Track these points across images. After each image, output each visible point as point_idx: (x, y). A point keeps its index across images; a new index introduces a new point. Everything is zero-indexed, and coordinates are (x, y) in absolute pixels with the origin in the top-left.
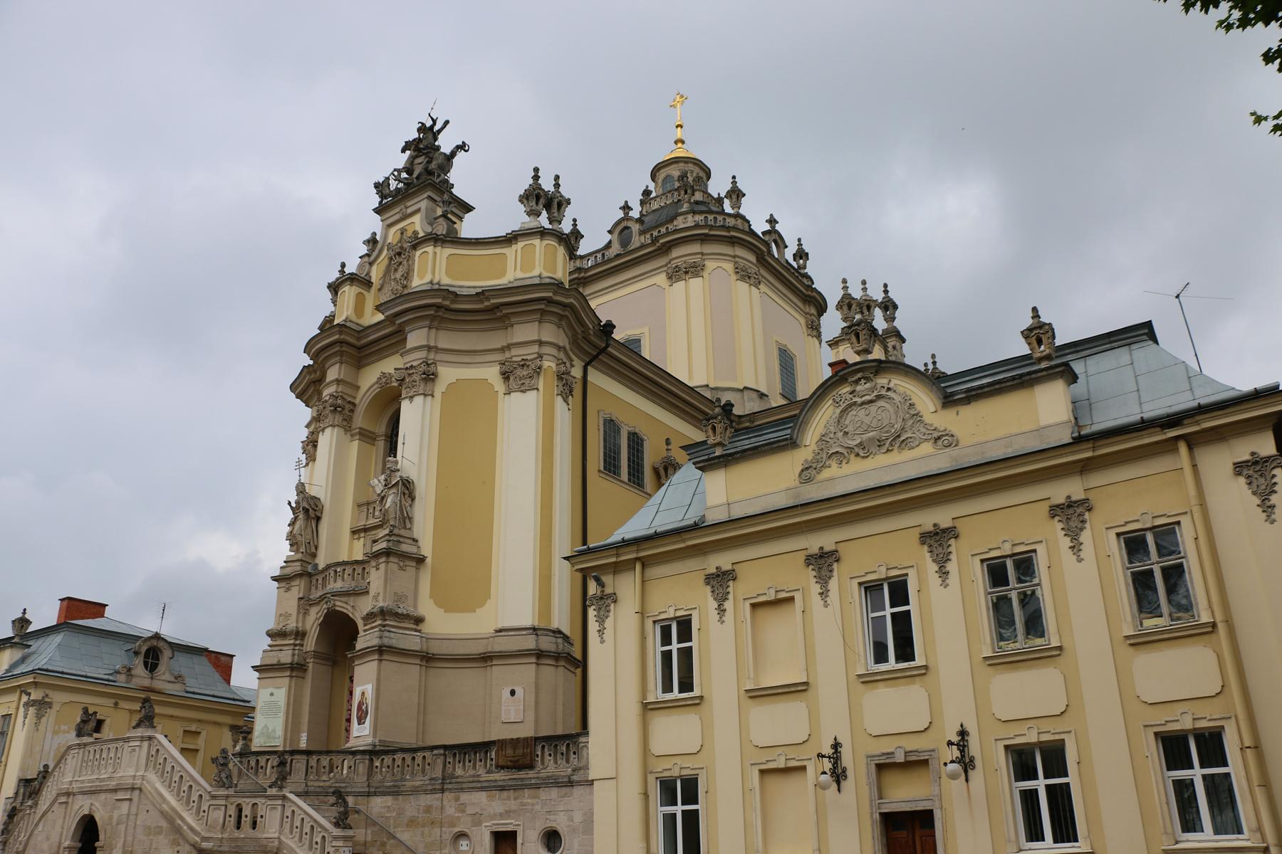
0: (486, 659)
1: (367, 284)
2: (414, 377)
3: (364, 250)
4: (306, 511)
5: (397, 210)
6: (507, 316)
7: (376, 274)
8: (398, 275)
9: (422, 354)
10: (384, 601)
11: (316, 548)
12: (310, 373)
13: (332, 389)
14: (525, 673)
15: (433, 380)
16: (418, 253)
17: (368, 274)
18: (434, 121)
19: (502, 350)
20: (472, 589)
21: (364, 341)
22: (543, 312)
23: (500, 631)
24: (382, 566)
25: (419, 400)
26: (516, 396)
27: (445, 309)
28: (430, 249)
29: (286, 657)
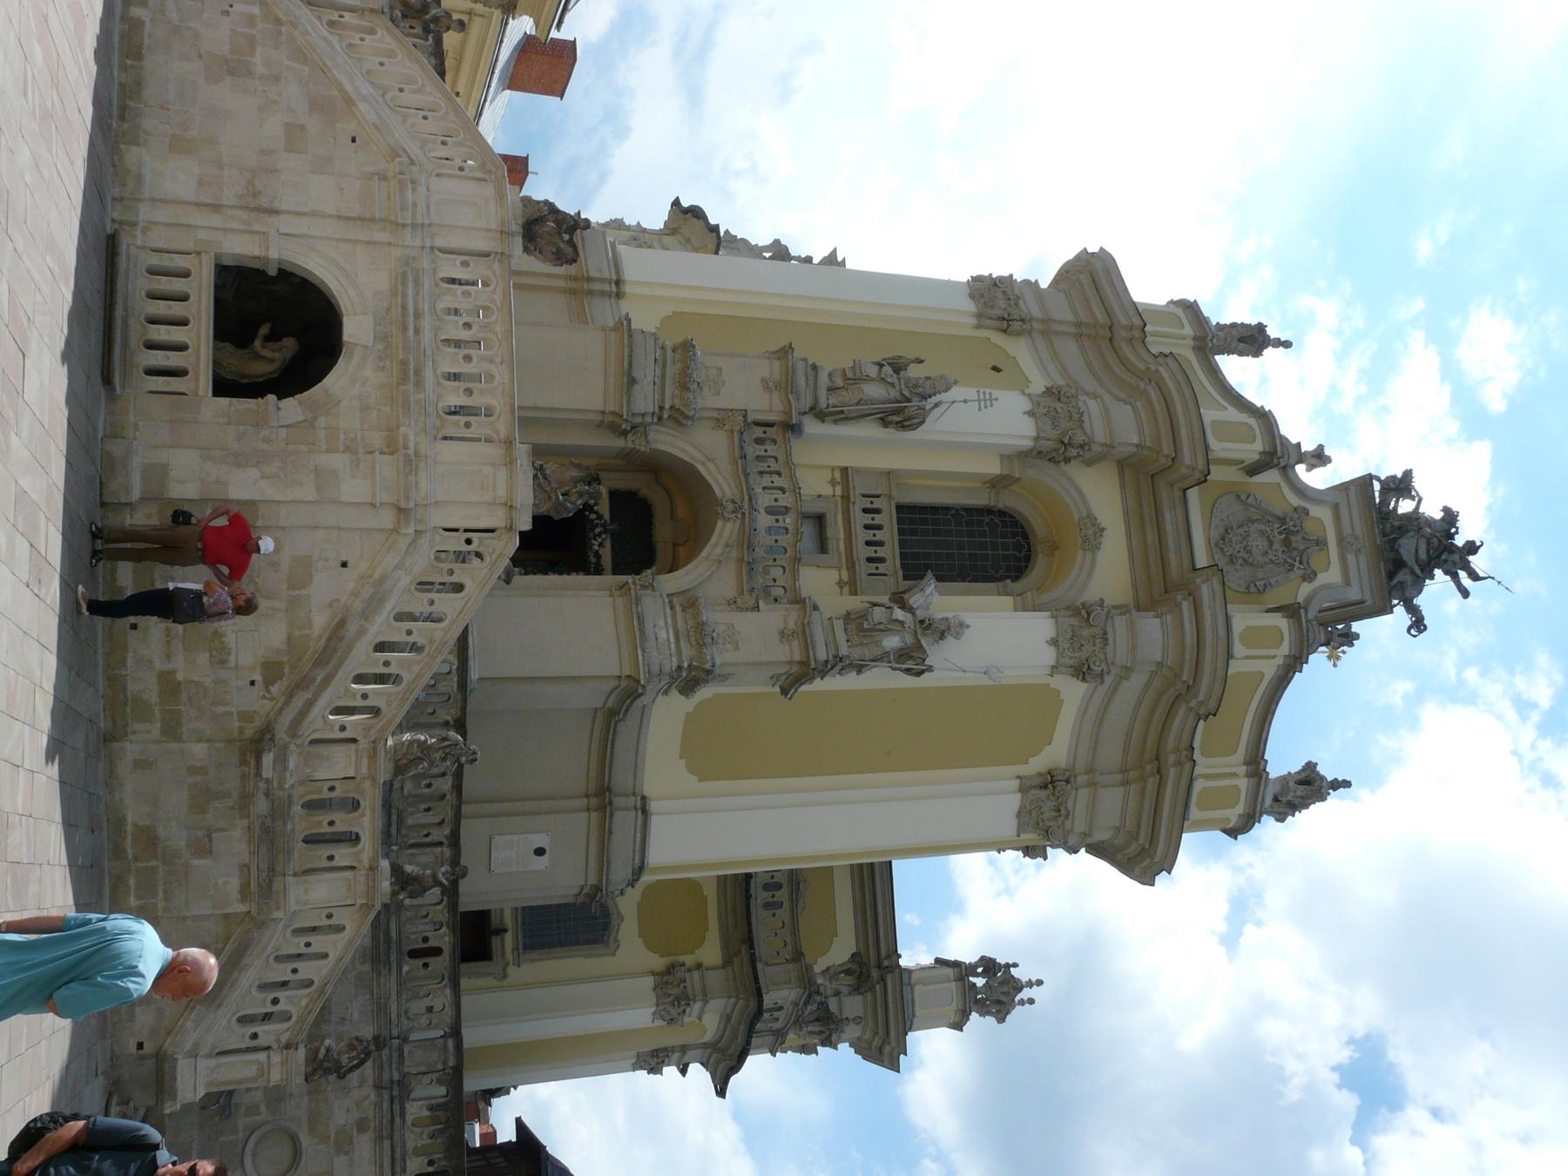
1: (1254, 470)
5: (1358, 530)
12: (1131, 328)
18: (1475, 577)
21: (1164, 494)
22: (1134, 836)
25: (1048, 656)
26: (1014, 801)
28: (1285, 649)
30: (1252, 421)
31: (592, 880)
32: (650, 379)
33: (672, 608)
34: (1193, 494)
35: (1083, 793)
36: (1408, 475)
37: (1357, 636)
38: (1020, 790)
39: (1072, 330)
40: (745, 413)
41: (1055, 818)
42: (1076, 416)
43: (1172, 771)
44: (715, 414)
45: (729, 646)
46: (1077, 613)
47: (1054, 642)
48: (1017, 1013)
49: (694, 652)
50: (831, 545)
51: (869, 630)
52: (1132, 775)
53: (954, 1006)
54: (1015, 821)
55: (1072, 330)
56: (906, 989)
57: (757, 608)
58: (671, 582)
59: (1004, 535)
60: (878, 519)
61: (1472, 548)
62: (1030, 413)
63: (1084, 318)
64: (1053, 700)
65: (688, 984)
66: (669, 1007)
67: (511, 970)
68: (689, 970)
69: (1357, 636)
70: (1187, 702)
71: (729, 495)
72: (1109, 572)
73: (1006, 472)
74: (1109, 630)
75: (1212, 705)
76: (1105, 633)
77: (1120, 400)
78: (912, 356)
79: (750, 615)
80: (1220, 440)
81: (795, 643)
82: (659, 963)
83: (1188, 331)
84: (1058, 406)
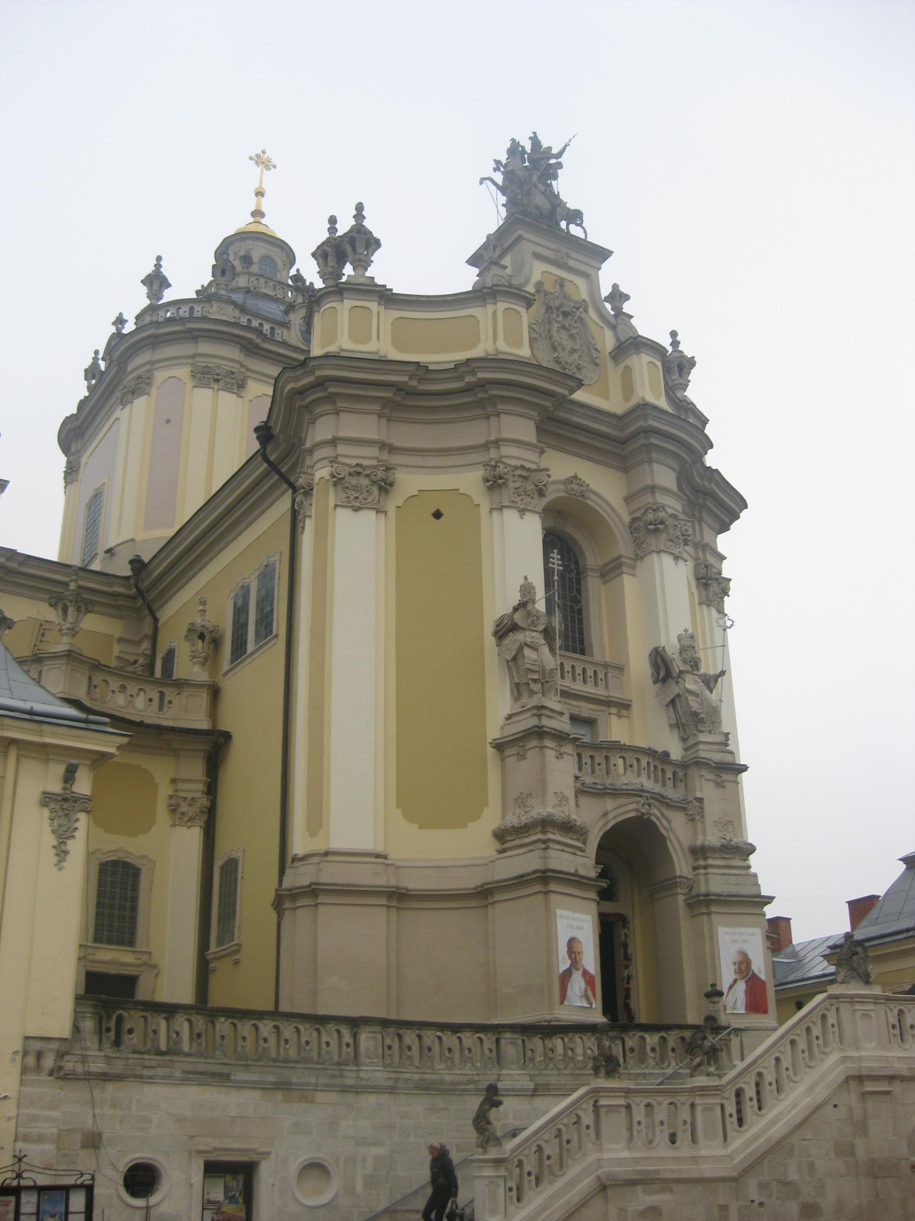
5: (553, 246)
12: (411, 377)
28: (659, 364)
30: (501, 306)
32: (572, 857)
33: (705, 867)
34: (580, 396)
35: (711, 559)
37: (615, 287)
39: (384, 421)
40: (577, 778)
41: (719, 583)
42: (524, 473)
45: (730, 829)
46: (656, 531)
47: (677, 558)
49: (738, 856)
50: (593, 715)
57: (700, 800)
58: (682, 866)
60: (567, 668)
62: (522, 512)
69: (615, 287)
71: (640, 806)
72: (604, 486)
74: (670, 511)
77: (488, 418)
78: (511, 610)
79: (707, 805)
80: (520, 345)
83: (373, 306)
84: (511, 485)
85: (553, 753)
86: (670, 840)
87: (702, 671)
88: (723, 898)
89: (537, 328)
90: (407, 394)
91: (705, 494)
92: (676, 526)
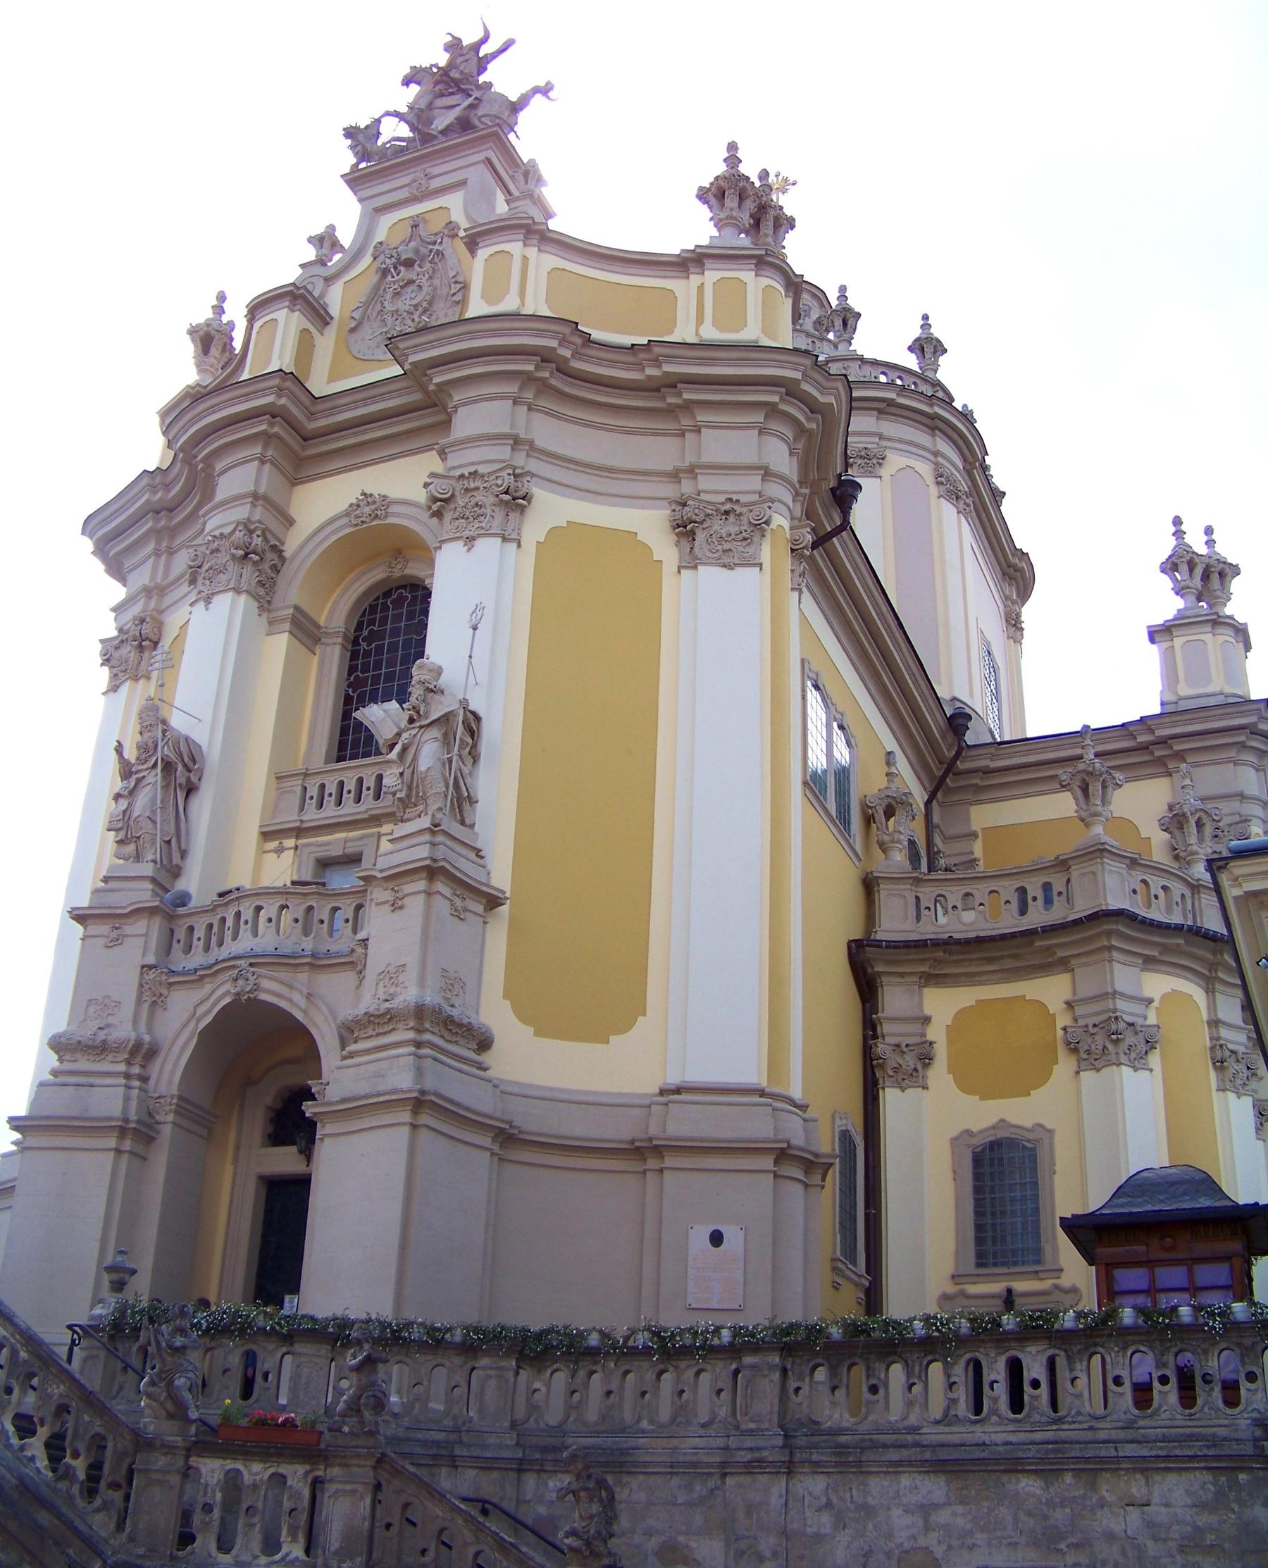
0: (645, 1152)
1: (321, 316)
2: (479, 497)
3: (310, 254)
4: (168, 767)
5: (406, 180)
6: (688, 406)
7: (336, 299)
8: (404, 304)
9: (503, 452)
10: (422, 982)
11: (184, 854)
12: (153, 489)
13: (242, 512)
14: (748, 1197)
15: (522, 509)
16: (483, 254)
17: (322, 295)
19: (675, 476)
20: (600, 987)
22: (772, 411)
23: (678, 1091)
24: (416, 905)
25: (488, 547)
27: (554, 366)
28: (515, 248)
29: (109, 1100)
31: (767, 1162)
36: (350, 133)
38: (695, 567)
43: (667, 368)
44: (146, 1006)
45: (402, 978)
48: (1227, 550)
49: (401, 1026)
50: (352, 849)
51: (410, 788)
52: (686, 421)
53: (1208, 638)
54: (740, 571)
55: (164, 558)
56: (1183, 705)
59: (383, 621)
61: (454, 46)
62: (208, 600)
63: (151, 547)
64: (567, 537)
65: (1091, 1021)
66: (1124, 1046)
67: (1065, 1281)
68: (1075, 1020)
70: (566, 360)
71: (228, 986)
73: (287, 626)
74: (457, 473)
75: (567, 330)
76: (462, 476)
78: (113, 756)
81: (408, 888)
82: (1065, 1065)
85: (101, 941)
86: (316, 1025)
87: (434, 716)
88: (333, 1108)
89: (357, 315)
90: (171, 510)
91: (675, 387)
92: (477, 489)
